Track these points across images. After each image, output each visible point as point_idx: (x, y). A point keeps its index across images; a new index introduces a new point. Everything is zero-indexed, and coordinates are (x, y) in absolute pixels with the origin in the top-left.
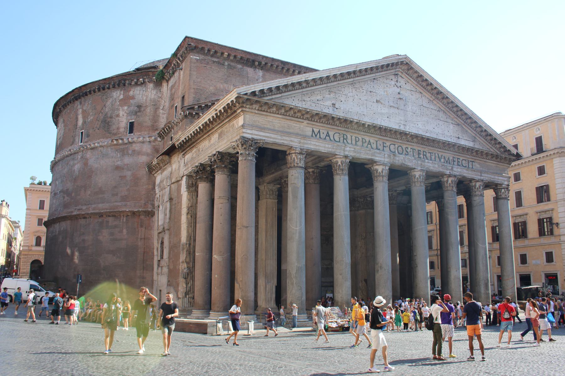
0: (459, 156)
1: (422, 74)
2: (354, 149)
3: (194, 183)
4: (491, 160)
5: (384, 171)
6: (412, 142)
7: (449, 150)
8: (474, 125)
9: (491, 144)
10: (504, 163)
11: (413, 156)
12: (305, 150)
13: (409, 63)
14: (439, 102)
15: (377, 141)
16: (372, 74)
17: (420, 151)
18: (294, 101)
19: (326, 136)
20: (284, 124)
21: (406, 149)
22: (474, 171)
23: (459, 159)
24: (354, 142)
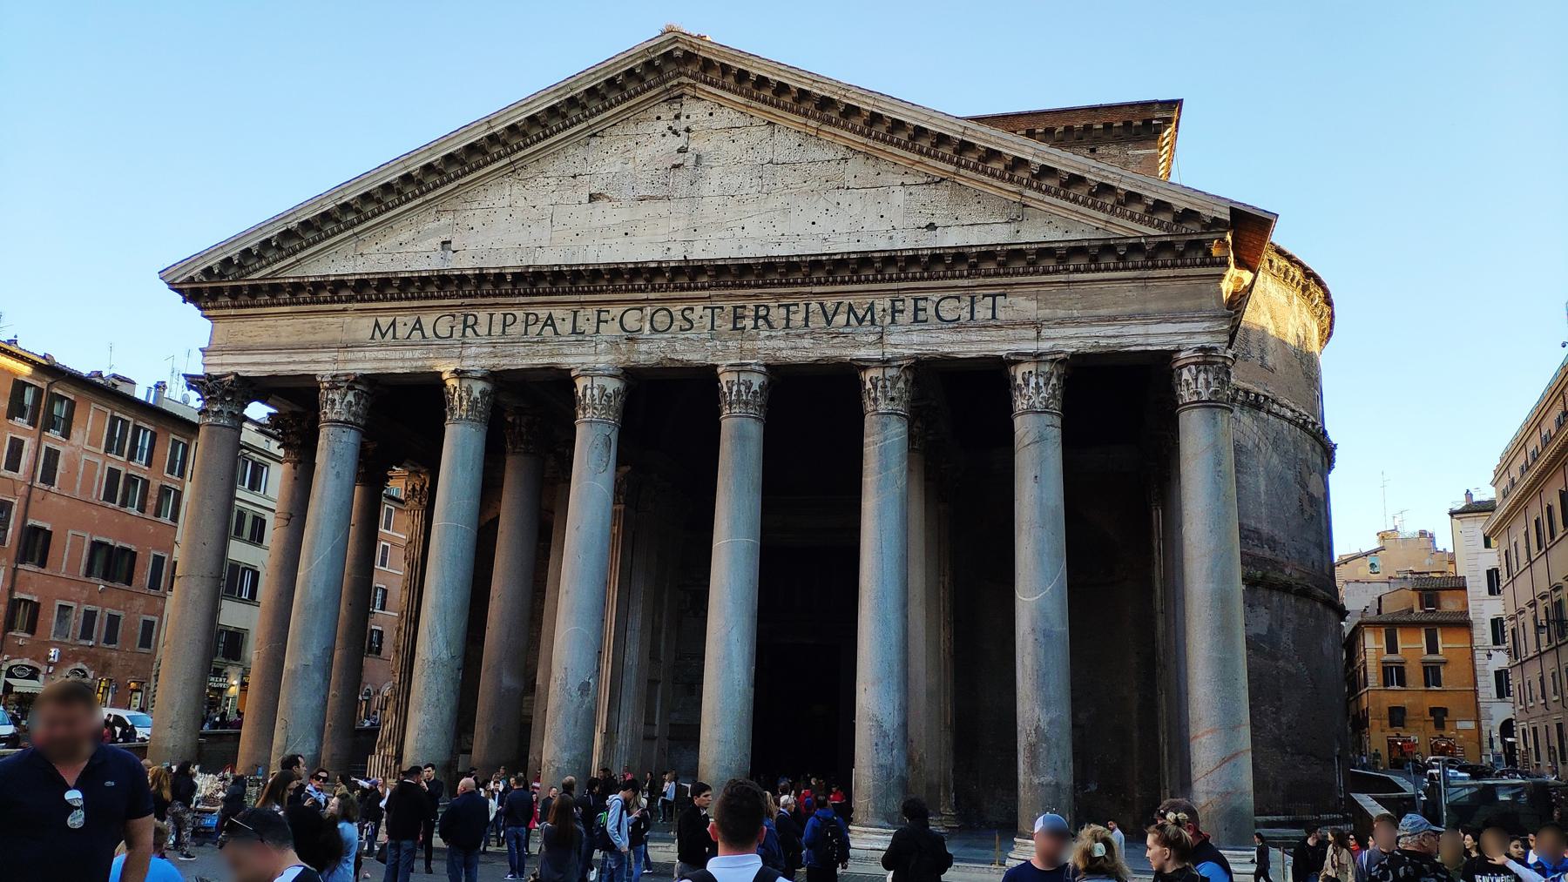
1: (741, 67)
2: (492, 349)
3: (418, 488)
4: (1098, 270)
5: (589, 392)
6: (696, 288)
7: (859, 282)
8: (998, 166)
9: (1103, 209)
10: (1184, 266)
11: (712, 328)
12: (344, 378)
13: (691, 50)
15: (575, 313)
16: (572, 124)
17: (744, 307)
19: (414, 329)
20: (305, 323)
21: (686, 313)
23: (926, 299)
24: (497, 329)
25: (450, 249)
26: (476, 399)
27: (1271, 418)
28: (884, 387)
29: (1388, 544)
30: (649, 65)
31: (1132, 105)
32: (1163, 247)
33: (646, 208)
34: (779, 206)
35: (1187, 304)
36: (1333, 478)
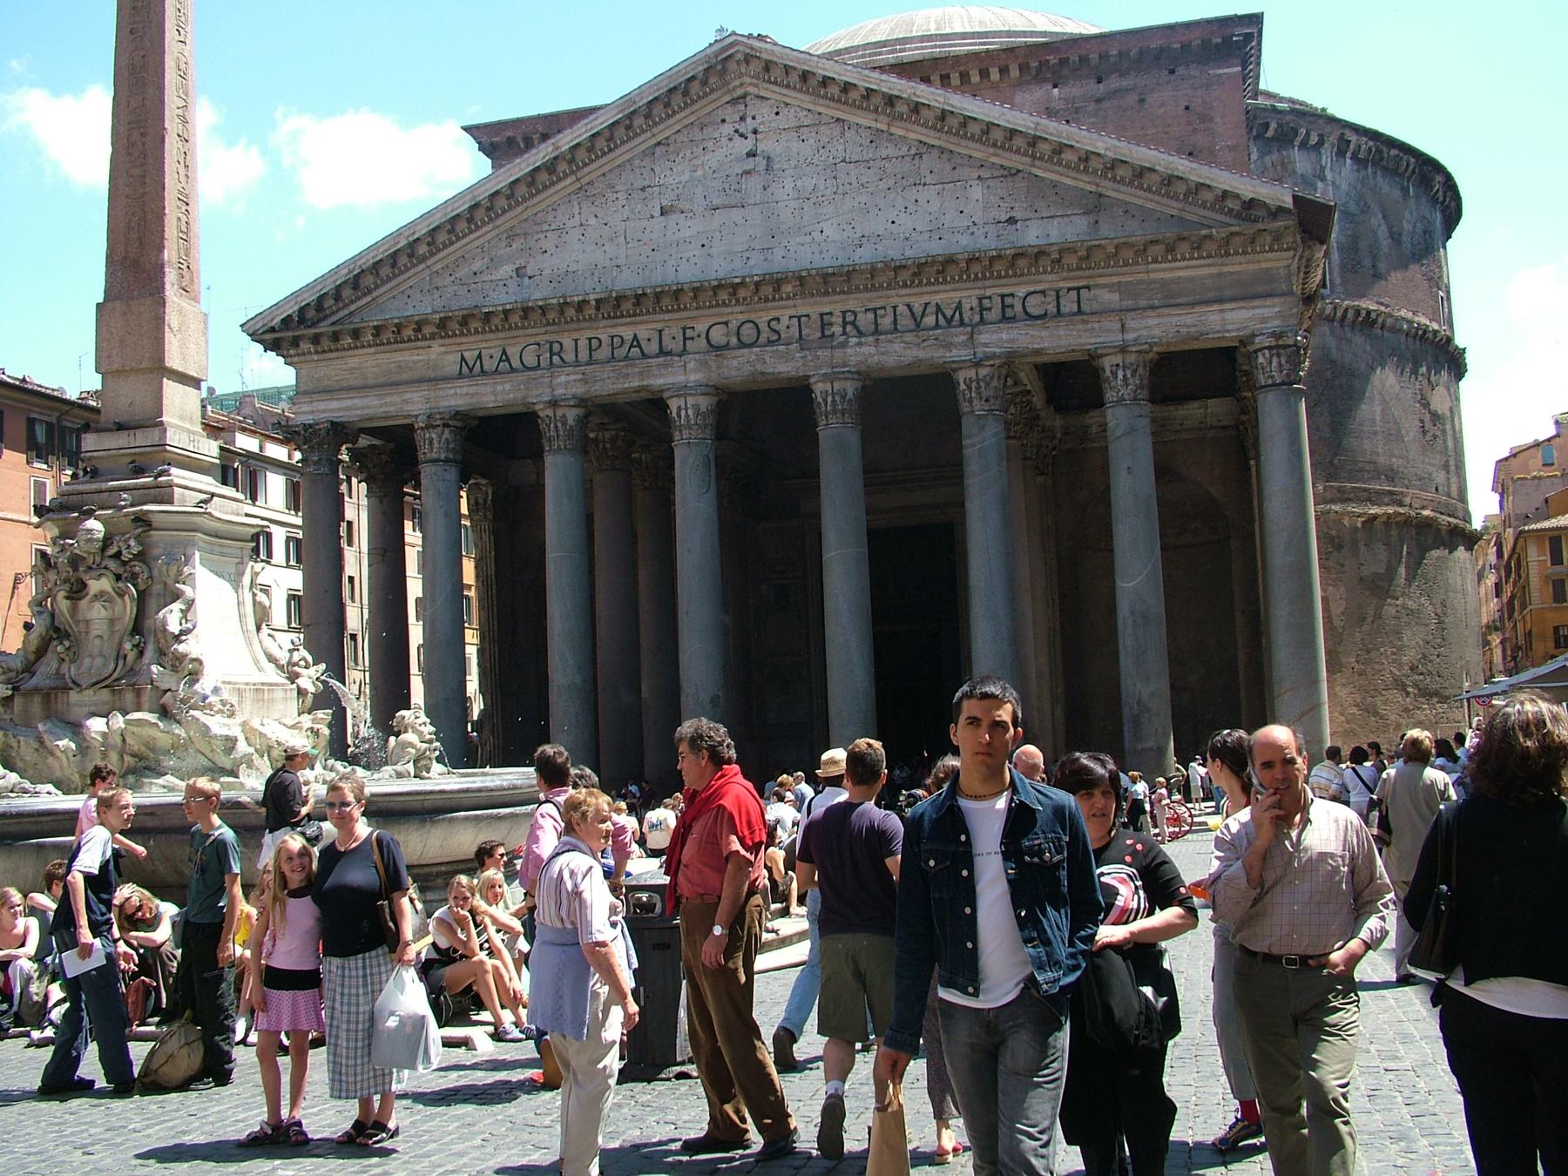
0: (1004, 285)
3: (481, 501)
5: (683, 413)
6: (782, 299)
7: (945, 282)
8: (1068, 156)
9: (1175, 198)
13: (753, 53)
14: (908, 125)
16: (636, 135)
17: (831, 314)
18: (409, 301)
19: (501, 361)
21: (773, 323)
22: (1084, 322)
23: (1012, 295)
24: (584, 355)
25: (525, 275)
26: (571, 427)
27: (1386, 334)
28: (978, 387)
29: (1564, 431)
30: (707, 70)
31: (1209, 22)
32: (1232, 234)
33: (720, 217)
34: (856, 204)
35: (1260, 289)
36: (1464, 384)
